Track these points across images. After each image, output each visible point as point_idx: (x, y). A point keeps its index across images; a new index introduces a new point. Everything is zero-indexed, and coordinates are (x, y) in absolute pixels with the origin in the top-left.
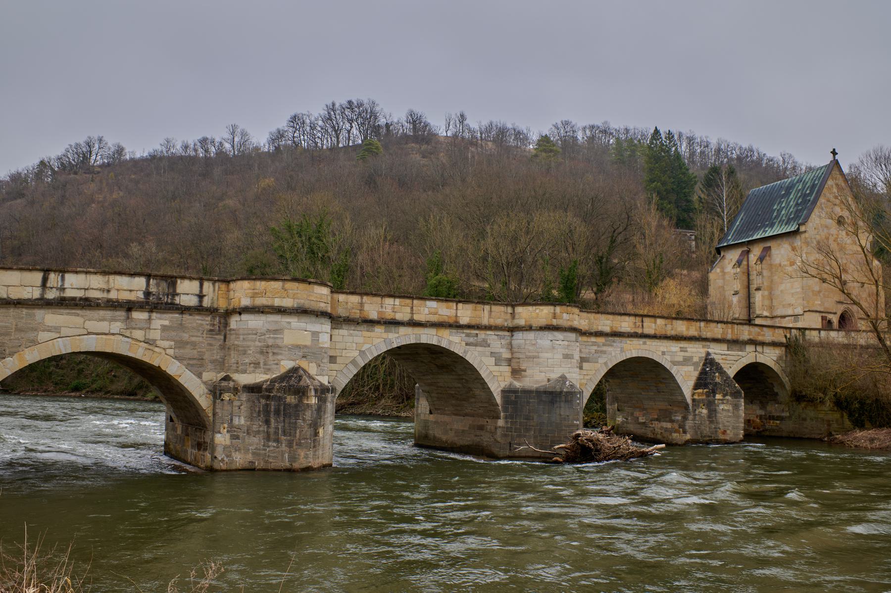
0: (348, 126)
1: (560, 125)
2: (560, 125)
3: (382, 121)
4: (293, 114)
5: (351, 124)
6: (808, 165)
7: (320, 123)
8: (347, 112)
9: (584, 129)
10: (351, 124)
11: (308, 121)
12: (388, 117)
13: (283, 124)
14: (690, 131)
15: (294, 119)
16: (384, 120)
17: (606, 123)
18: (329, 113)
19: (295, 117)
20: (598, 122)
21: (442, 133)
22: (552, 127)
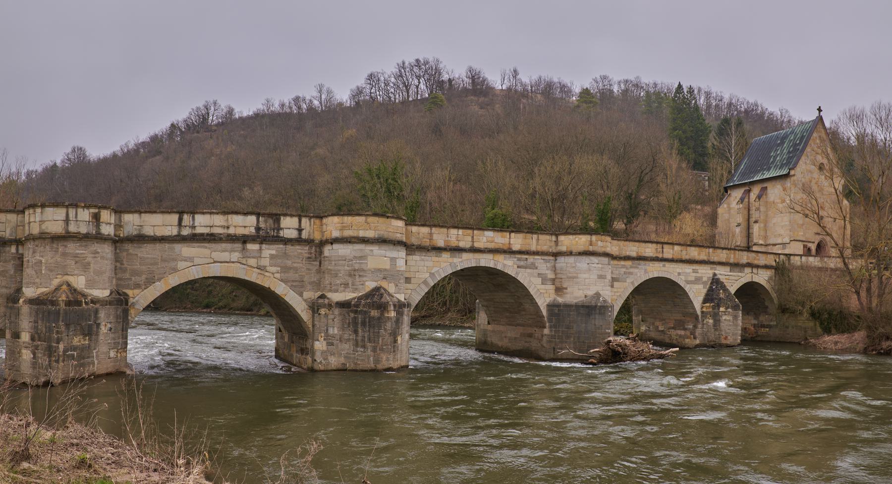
1: (599, 79)
2: (599, 79)
6: (800, 120)
9: (619, 83)
17: (638, 77)
20: (631, 77)
21: (498, 86)
22: (591, 80)
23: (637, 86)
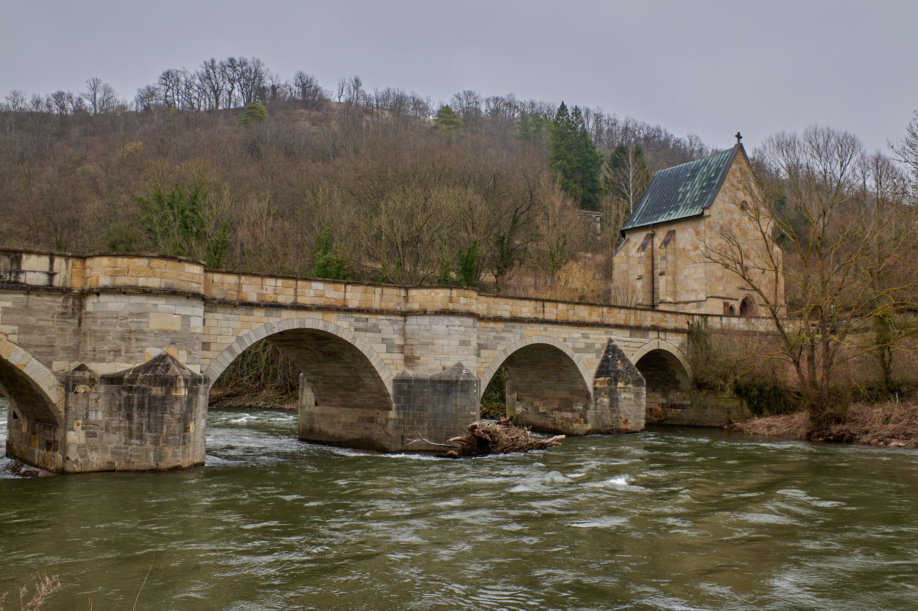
0: (229, 86)
1: (462, 95)
2: (462, 95)
3: (268, 83)
4: (165, 70)
5: (232, 85)
6: (714, 148)
7: (197, 81)
8: (229, 71)
9: (488, 100)
10: (232, 85)
11: (183, 79)
12: (274, 79)
13: (153, 80)
14: (598, 107)
15: (167, 75)
16: (270, 81)
17: (511, 95)
18: (207, 71)
19: (168, 73)
20: (503, 95)
22: (453, 97)
23: (509, 105)
